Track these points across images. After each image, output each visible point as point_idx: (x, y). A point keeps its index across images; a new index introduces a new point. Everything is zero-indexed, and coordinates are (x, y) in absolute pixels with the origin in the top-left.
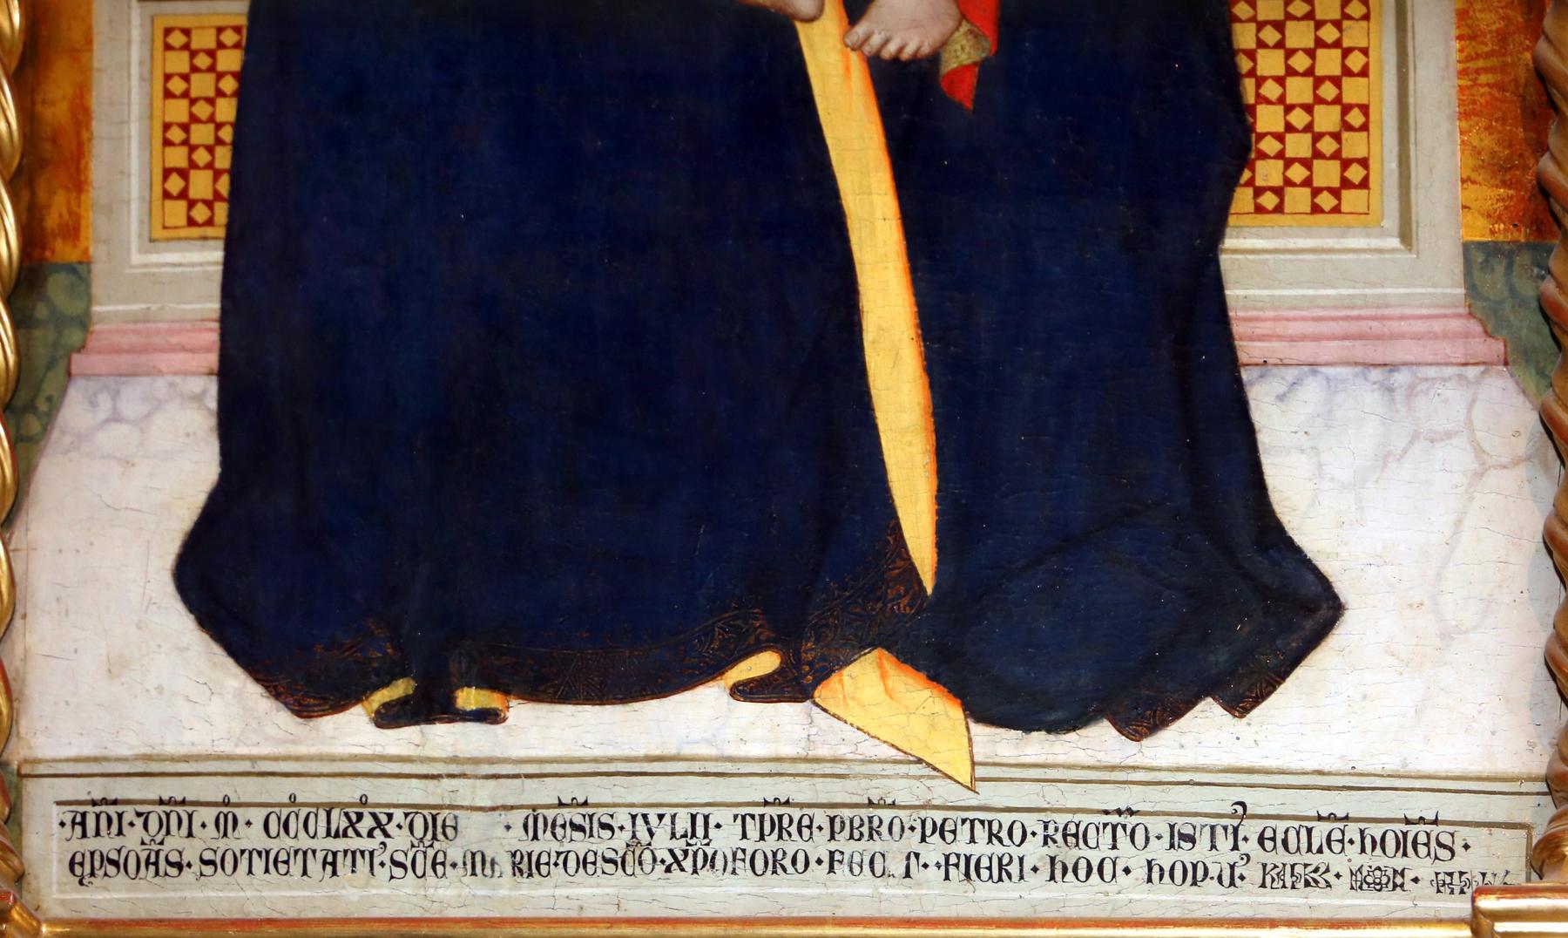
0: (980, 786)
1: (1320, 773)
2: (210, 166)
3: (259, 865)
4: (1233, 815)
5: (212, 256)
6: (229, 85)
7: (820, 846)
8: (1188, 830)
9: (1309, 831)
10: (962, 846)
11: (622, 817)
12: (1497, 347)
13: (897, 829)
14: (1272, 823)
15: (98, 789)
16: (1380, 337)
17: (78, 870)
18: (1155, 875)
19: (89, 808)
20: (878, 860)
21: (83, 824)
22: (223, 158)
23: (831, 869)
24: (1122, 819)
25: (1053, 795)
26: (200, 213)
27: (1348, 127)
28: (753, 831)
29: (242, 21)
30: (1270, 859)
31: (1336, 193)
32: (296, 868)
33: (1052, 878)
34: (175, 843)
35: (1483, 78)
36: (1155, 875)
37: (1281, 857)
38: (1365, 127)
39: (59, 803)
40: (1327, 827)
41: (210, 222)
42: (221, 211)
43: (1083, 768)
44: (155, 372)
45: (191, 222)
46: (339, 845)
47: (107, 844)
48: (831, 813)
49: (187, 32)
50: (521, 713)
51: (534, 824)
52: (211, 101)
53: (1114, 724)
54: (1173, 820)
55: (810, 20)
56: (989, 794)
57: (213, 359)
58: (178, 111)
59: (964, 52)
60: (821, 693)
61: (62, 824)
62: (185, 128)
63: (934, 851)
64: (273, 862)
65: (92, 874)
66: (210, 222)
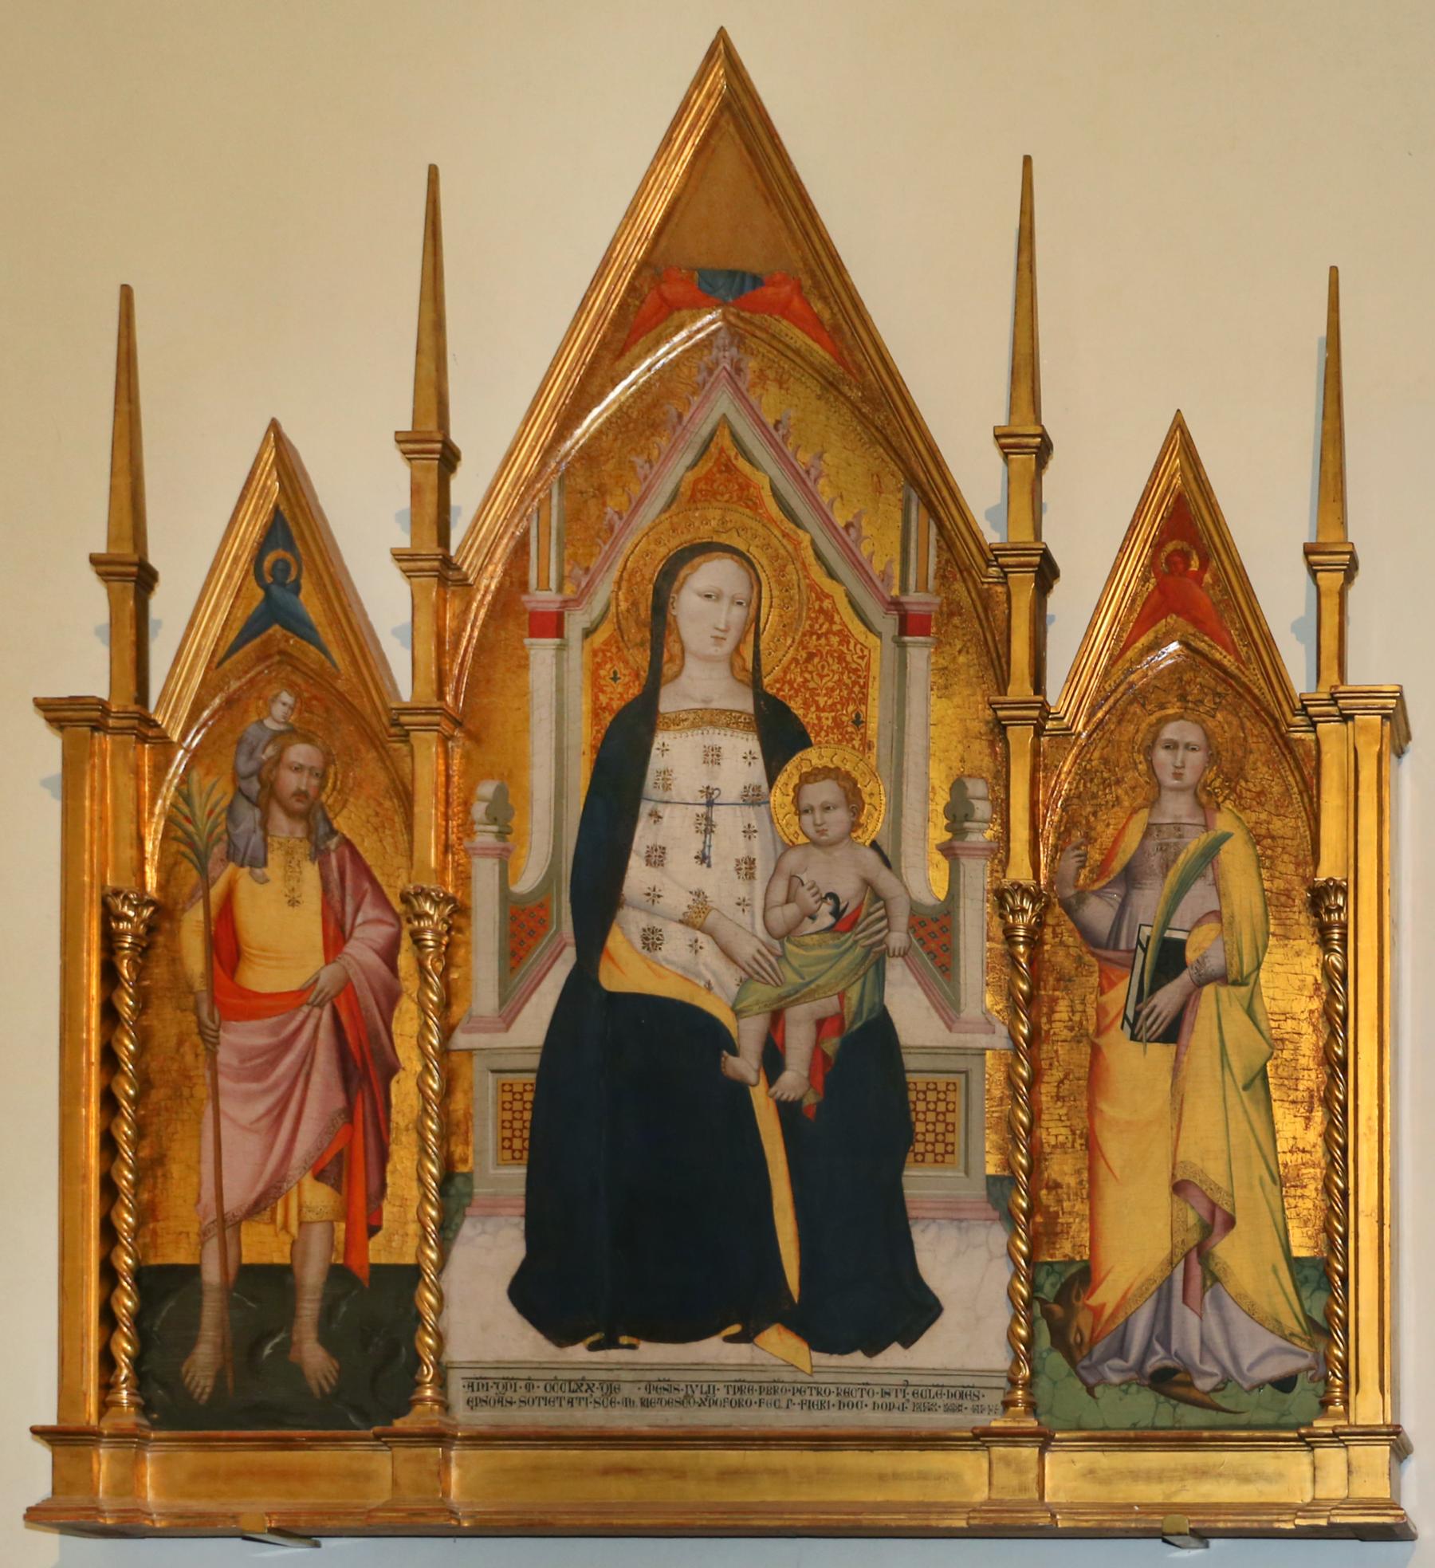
2: (521, 1137)
3: (542, 1403)
5: (523, 1171)
6: (528, 1106)
7: (755, 1397)
10: (807, 1397)
11: (682, 1386)
15: (478, 1373)
22: (526, 1134)
26: (517, 1155)
28: (731, 1392)
29: (533, 1081)
32: (557, 1404)
34: (509, 1394)
41: (521, 1158)
42: (526, 1154)
44: (497, 1215)
45: (514, 1158)
46: (573, 1395)
47: (482, 1394)
49: (511, 1085)
50: (644, 1346)
51: (648, 1389)
52: (521, 1112)
56: (818, 1378)
57: (522, 1210)
58: (508, 1116)
60: (756, 1340)
62: (511, 1122)
63: (797, 1399)
64: (548, 1401)
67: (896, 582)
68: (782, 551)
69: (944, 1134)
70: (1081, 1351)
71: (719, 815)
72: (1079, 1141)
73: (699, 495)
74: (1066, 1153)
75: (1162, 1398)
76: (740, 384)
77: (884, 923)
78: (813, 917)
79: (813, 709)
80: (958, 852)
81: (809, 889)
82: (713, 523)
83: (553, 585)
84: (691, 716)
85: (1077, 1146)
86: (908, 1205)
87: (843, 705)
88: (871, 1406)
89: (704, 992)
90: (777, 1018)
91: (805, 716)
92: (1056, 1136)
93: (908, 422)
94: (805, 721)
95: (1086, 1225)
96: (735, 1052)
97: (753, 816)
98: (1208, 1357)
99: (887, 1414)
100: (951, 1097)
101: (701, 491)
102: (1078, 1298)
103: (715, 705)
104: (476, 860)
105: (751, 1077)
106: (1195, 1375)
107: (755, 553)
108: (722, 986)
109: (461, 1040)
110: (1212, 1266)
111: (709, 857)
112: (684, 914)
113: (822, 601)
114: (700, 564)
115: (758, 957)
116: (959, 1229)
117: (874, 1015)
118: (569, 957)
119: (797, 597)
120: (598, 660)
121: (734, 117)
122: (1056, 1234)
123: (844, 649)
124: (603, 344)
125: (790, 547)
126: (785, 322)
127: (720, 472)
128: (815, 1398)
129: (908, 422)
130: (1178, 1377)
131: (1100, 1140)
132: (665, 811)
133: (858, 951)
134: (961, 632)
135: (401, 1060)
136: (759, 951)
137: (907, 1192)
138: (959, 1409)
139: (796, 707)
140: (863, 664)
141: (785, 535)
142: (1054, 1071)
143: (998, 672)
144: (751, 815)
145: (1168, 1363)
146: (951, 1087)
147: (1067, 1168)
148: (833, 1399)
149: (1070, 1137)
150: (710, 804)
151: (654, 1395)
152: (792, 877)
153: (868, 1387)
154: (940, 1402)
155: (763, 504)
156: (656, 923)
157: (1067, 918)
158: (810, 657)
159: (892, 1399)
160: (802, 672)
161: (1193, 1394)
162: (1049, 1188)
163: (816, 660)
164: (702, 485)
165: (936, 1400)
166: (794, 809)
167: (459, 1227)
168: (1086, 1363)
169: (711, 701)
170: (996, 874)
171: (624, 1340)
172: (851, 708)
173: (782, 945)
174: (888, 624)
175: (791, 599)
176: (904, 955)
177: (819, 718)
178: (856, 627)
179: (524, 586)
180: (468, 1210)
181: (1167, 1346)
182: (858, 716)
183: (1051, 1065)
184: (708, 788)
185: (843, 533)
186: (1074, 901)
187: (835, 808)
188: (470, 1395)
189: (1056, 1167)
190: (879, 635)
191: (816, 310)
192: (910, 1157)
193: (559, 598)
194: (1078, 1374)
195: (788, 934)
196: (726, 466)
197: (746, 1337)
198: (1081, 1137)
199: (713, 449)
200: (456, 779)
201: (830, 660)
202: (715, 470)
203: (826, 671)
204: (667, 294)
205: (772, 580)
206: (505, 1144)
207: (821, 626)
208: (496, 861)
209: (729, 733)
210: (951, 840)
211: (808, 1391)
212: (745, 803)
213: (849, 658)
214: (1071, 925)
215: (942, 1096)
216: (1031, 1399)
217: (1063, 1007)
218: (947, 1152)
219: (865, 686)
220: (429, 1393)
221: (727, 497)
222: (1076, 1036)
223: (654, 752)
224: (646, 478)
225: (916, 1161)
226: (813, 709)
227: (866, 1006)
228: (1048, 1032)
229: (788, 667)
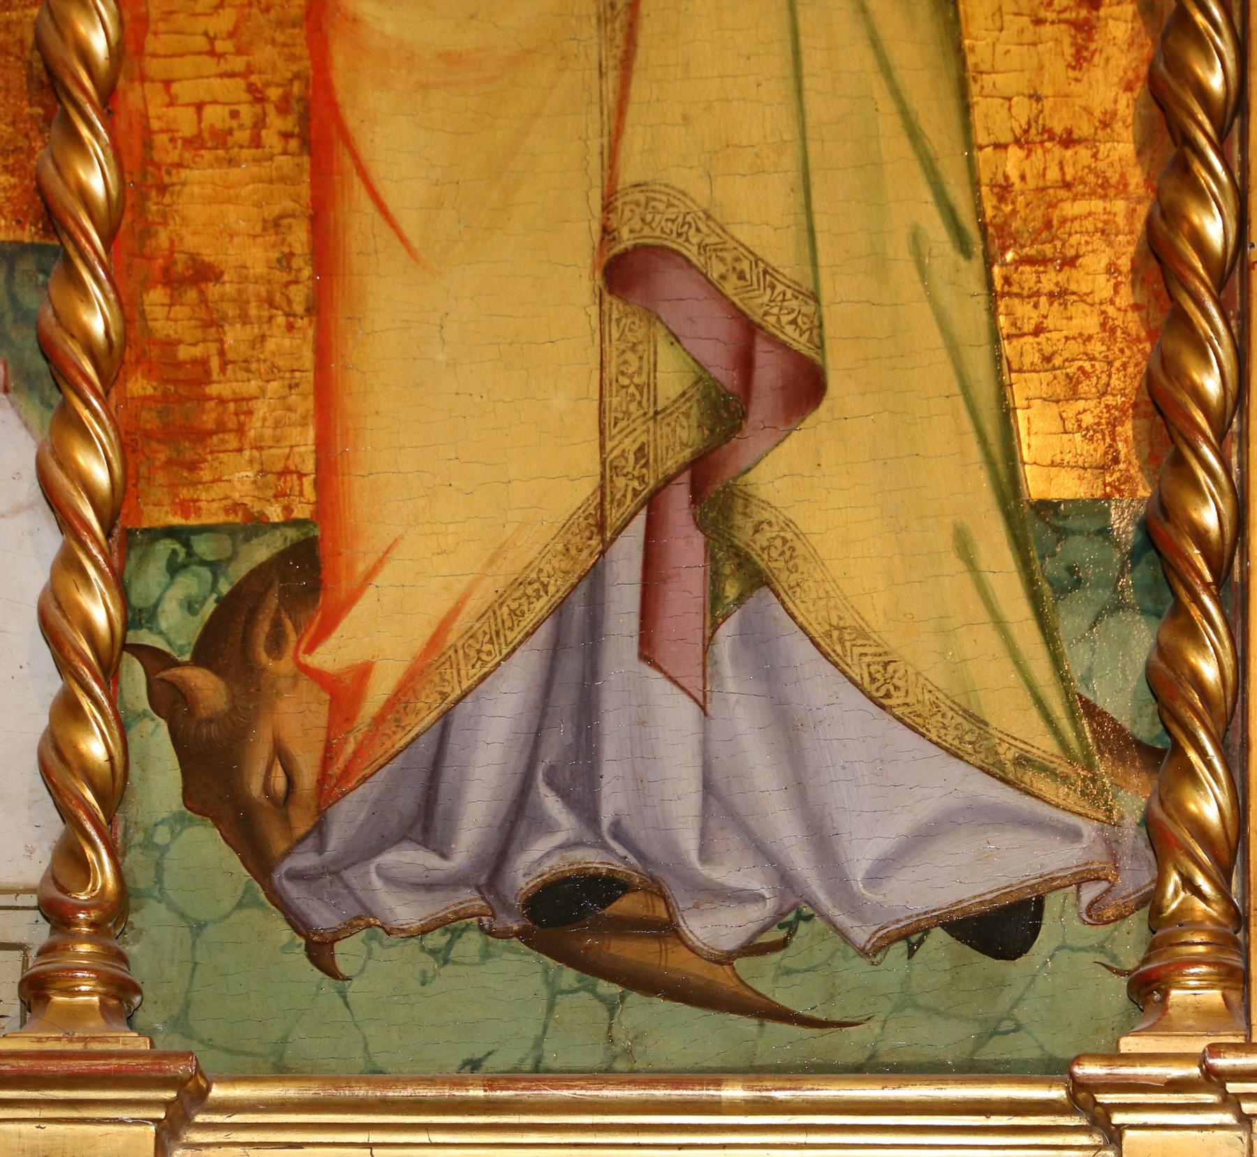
70: (286, 820)
72: (276, 123)
74: (231, 162)
75: (569, 976)
85: (270, 138)
92: (199, 107)
95: (307, 405)
98: (727, 841)
102: (276, 643)
106: (682, 901)
110: (743, 537)
122: (201, 436)
130: (626, 905)
131: (352, 120)
145: (592, 859)
161: (677, 962)
162: (173, 282)
168: (304, 860)
181: (586, 809)
198: (283, 108)
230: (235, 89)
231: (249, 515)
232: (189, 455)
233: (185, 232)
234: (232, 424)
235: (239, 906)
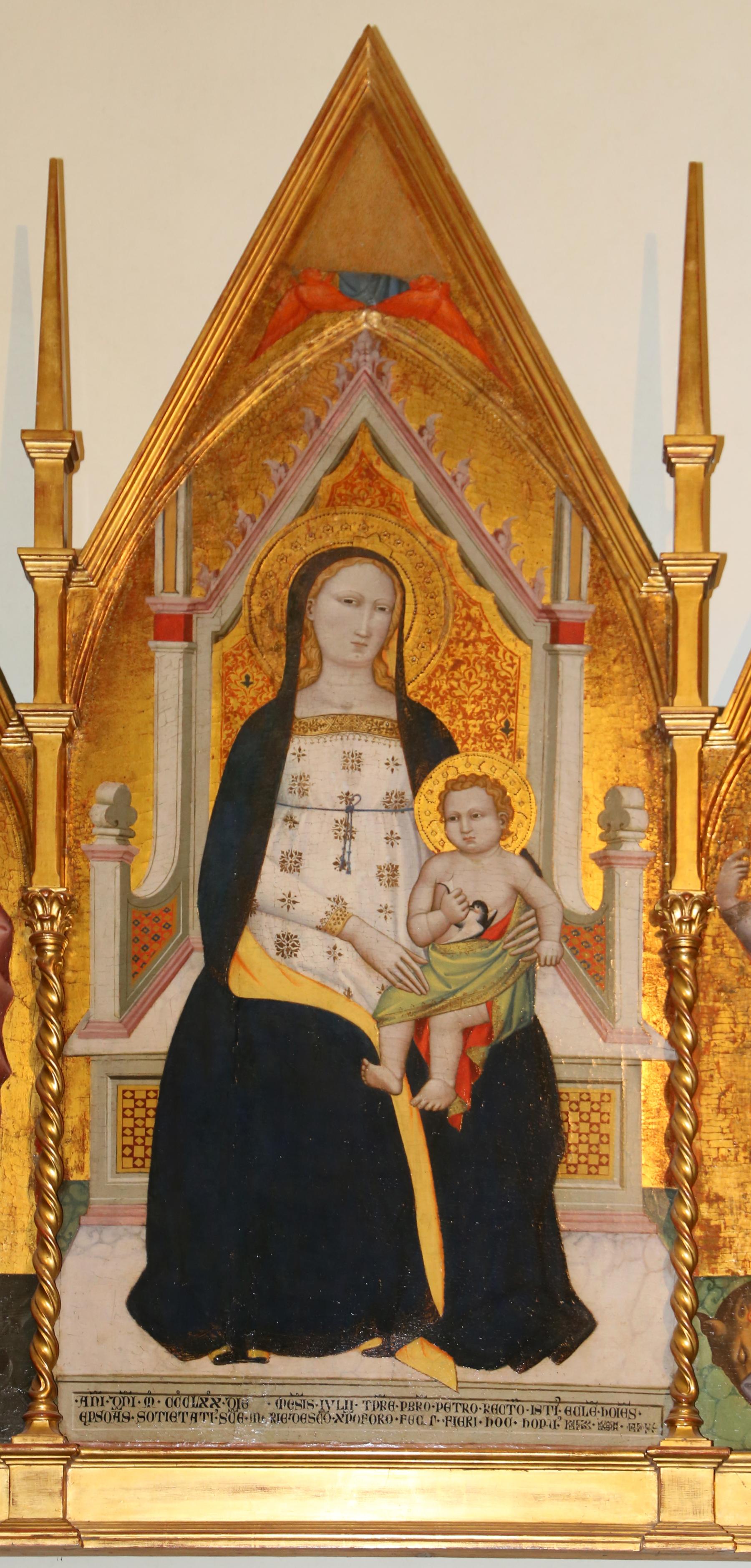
0: (460, 1390)
1: (588, 1386)
2: (143, 1144)
3: (163, 1418)
4: (556, 1402)
5: (143, 1180)
6: (152, 1113)
7: (397, 1413)
8: (539, 1408)
9: (583, 1408)
10: (452, 1413)
11: (317, 1401)
12: (653, 1227)
13: (427, 1406)
14: (569, 1405)
16: (613, 1222)
17: (83, 1419)
18: (526, 1424)
19: (89, 1395)
20: (420, 1419)
21: (86, 1401)
22: (149, 1141)
23: (401, 1422)
24: (514, 1403)
25: (486, 1394)
26: (139, 1163)
27: (602, 1142)
29: (158, 1088)
30: (569, 1418)
31: (596, 1167)
32: (179, 1419)
33: (487, 1425)
34: (127, 1409)
35: (650, 1127)
36: (526, 1424)
37: (573, 1418)
38: (608, 1143)
39: (75, 1393)
40: (589, 1406)
41: (143, 1166)
42: (148, 1162)
43: (500, 1383)
45: (135, 1166)
46: (198, 1410)
48: (402, 1400)
49: (133, 1092)
51: (279, 1403)
52: (144, 1119)
53: (512, 1367)
54: (533, 1404)
55: (397, 1094)
56: (463, 1394)
57: (144, 1220)
58: (129, 1123)
59: (457, 1109)
61: (76, 1401)
62: (132, 1129)
63: (441, 1415)
64: (170, 1417)
65: (90, 1421)
66: (143, 1166)
67: (548, 590)
68: (427, 558)
69: (597, 1146)
71: (359, 821)
72: (742, 1155)
73: (338, 500)
74: (728, 1166)
76: (382, 388)
77: (535, 931)
78: (459, 926)
79: (460, 716)
80: (613, 861)
81: (456, 897)
82: (354, 528)
83: (180, 587)
84: (330, 722)
85: (741, 1158)
86: (560, 1217)
87: (491, 713)
88: (521, 1423)
89: (343, 999)
90: (421, 1026)
91: (451, 723)
92: (718, 1149)
93: (566, 430)
94: (451, 728)
96: (376, 1061)
97: (396, 822)
99: (539, 1431)
100: (605, 1108)
101: (340, 495)
103: (354, 711)
104: (94, 863)
105: (394, 1086)
107: (400, 559)
108: (361, 992)
109: (76, 1045)
111: (349, 863)
112: (321, 920)
113: (469, 608)
114: (339, 569)
115: (402, 965)
116: (615, 1242)
117: (524, 1025)
118: (196, 965)
119: (443, 604)
120: (228, 664)
121: (378, 119)
122: (718, 1249)
123: (493, 656)
124: (237, 345)
125: (436, 554)
126: (432, 327)
127: (361, 476)
128: (460, 1414)
129: (566, 430)
132: (302, 817)
133: (508, 960)
134: (616, 641)
135: (12, 1066)
136: (402, 959)
137: (559, 1204)
138: (614, 1427)
139: (442, 714)
140: (513, 671)
141: (430, 541)
142: (715, 1083)
143: (656, 682)
144: (394, 821)
146: (606, 1098)
147: (731, 1181)
148: (480, 1415)
149: (733, 1151)
150: (350, 810)
151: (285, 1410)
152: (437, 884)
153: (517, 1404)
154: (594, 1419)
155: (406, 511)
156: (292, 929)
157: (728, 929)
158: (457, 664)
159: (543, 1416)
160: (448, 679)
162: (710, 1202)
163: (463, 668)
164: (342, 490)
165: (590, 1418)
166: (439, 816)
167: (73, 1236)
169: (351, 706)
170: (652, 885)
171: (253, 1353)
172: (500, 716)
173: (427, 953)
174: (540, 632)
175: (437, 605)
176: (556, 964)
177: (466, 726)
178: (506, 637)
179: (149, 588)
180: (83, 1219)
182: (507, 723)
183: (712, 1076)
184: (348, 794)
185: (492, 540)
186: (735, 912)
187: (483, 815)
188: (83, 1409)
189: (717, 1180)
190: (529, 643)
191: (465, 316)
192: (562, 1168)
193: (187, 601)
194: (742, 1393)
195: (433, 941)
196: (367, 470)
197: (386, 1351)
198: (745, 1149)
199: (354, 454)
200: (73, 781)
201: (478, 668)
202: (356, 474)
203: (473, 679)
204: (305, 296)
205: (417, 587)
206: (126, 1151)
207: (469, 634)
208: (118, 864)
209: (370, 739)
210: (605, 850)
211: (453, 1408)
212: (387, 809)
213: (497, 666)
214: (733, 936)
215: (596, 1107)
216: (695, 1417)
217: (724, 1017)
218: (601, 1164)
219: (515, 694)
220: (43, 1407)
221: (368, 502)
222: (738, 1047)
223: (290, 757)
224: (280, 481)
225: (569, 1172)
226: (460, 716)
227: (516, 1016)
228: (708, 1043)
229: (434, 674)
230: (729, 1144)
231: (733, 1273)
232: (714, 1254)
233: (713, 1186)
234: (728, 1245)
235: (730, 1394)
